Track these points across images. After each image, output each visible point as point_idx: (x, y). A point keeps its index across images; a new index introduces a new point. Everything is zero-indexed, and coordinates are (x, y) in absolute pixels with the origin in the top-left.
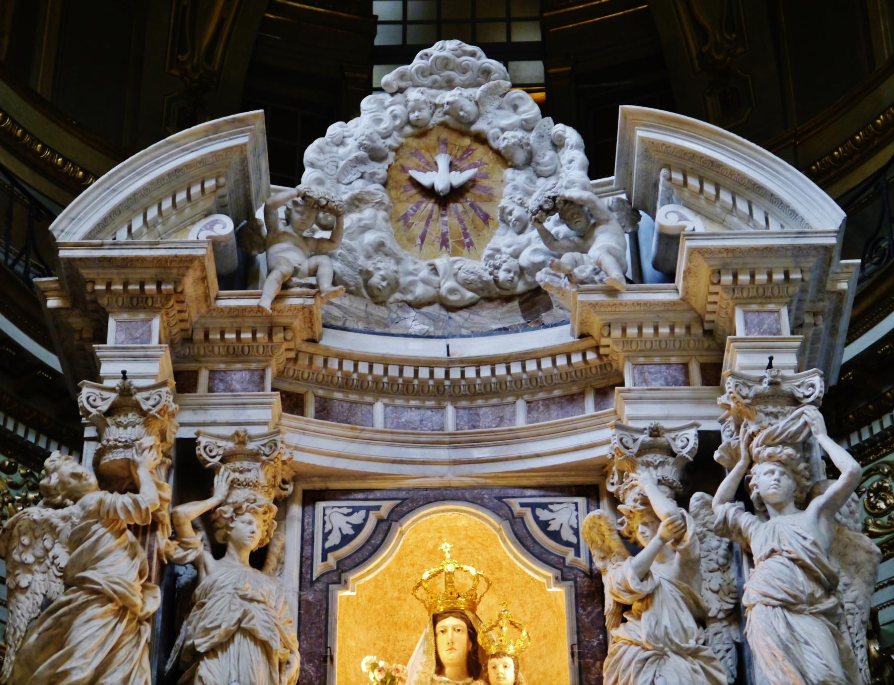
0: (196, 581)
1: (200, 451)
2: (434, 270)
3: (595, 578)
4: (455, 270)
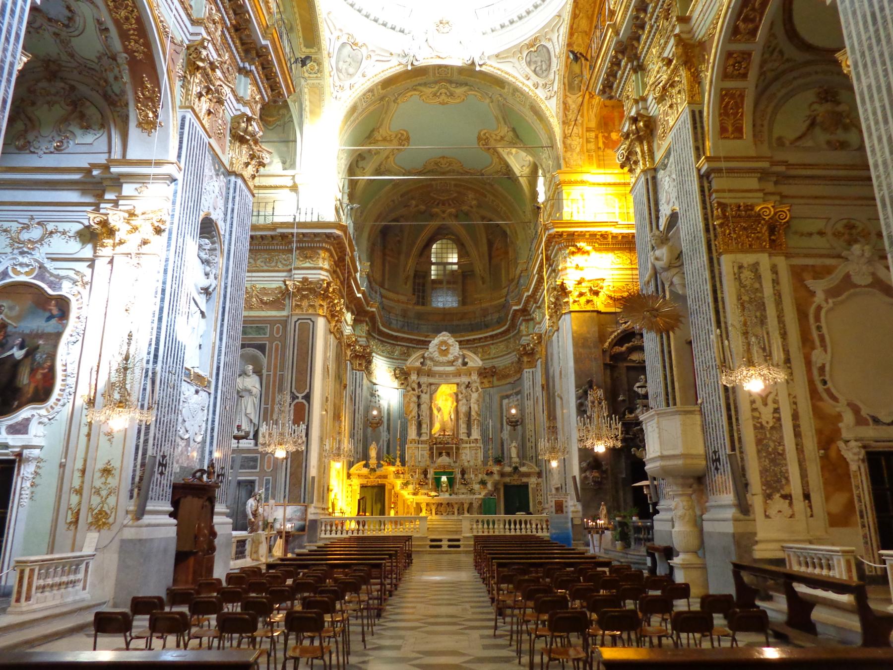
4: (444, 359)
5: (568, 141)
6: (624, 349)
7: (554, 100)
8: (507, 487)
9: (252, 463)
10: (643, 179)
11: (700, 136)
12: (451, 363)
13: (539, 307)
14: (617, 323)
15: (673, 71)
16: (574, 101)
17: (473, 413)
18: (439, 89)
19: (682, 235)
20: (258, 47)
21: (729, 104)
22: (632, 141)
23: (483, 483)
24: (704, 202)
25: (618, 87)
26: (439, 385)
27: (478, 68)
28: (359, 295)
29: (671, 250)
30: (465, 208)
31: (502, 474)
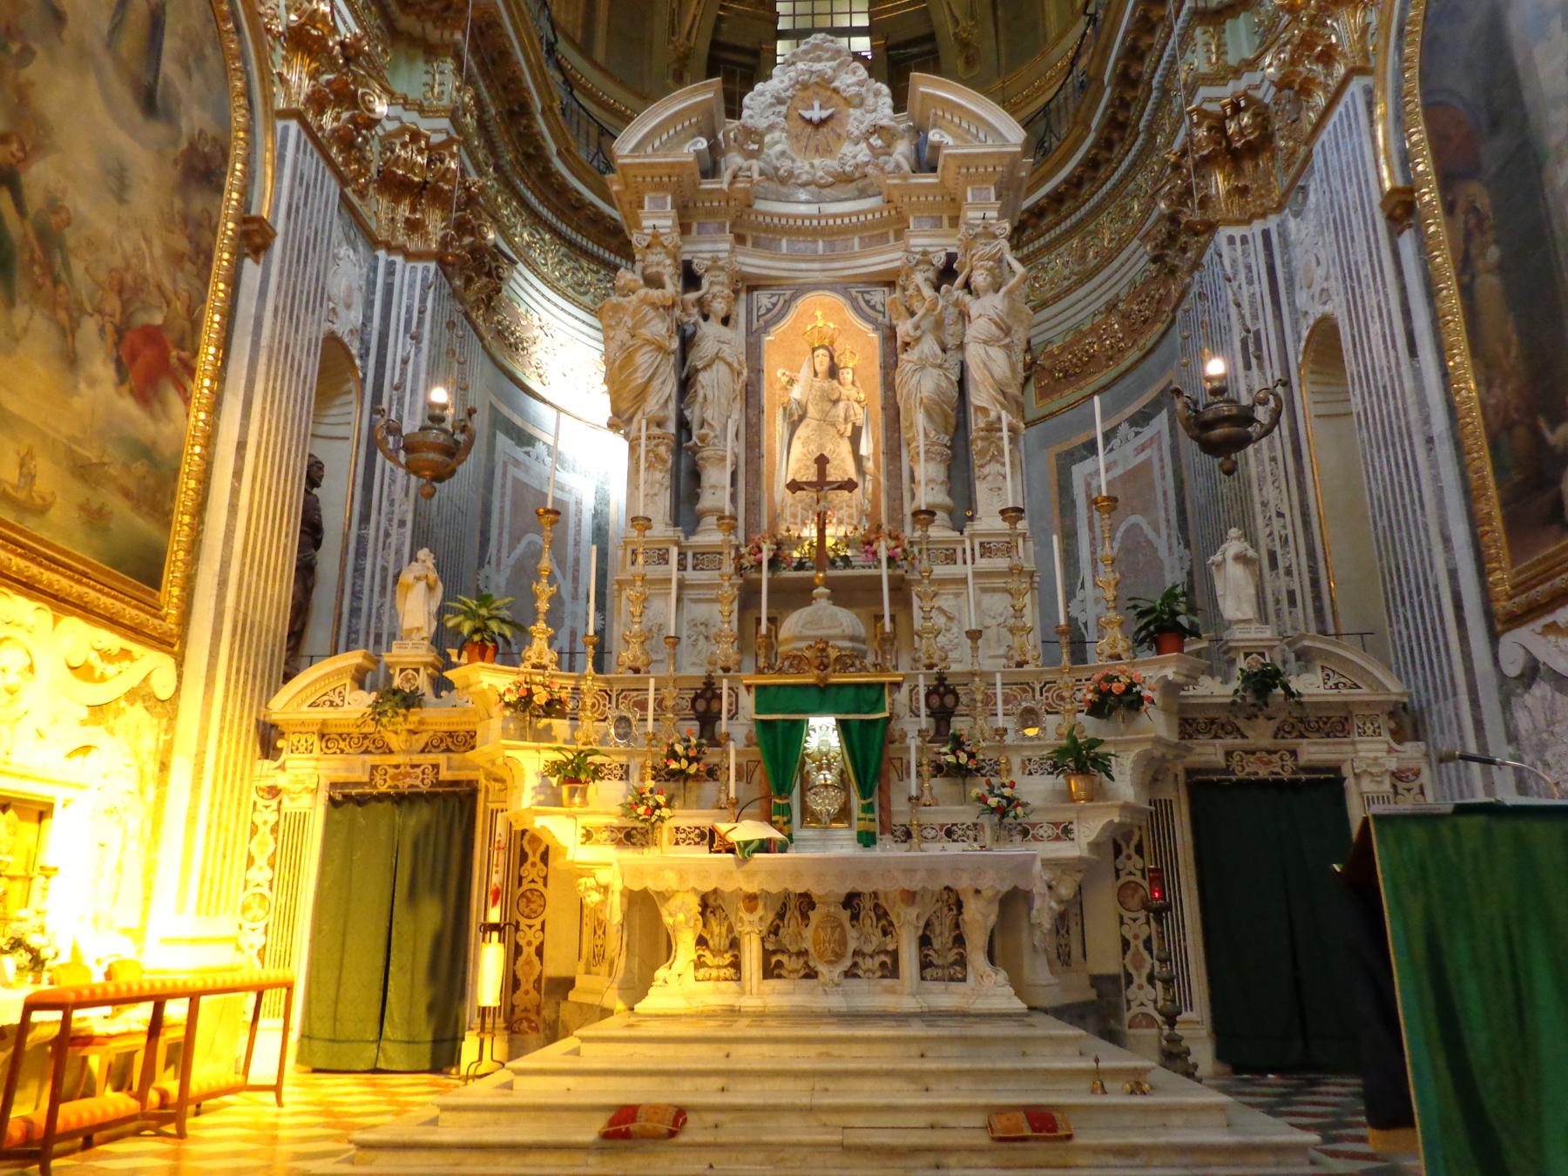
0: (694, 333)
1: (694, 266)
2: (812, 166)
3: (893, 329)
4: (823, 166)
17: (980, 396)
23: (1080, 760)
26: (801, 289)
31: (1191, 722)
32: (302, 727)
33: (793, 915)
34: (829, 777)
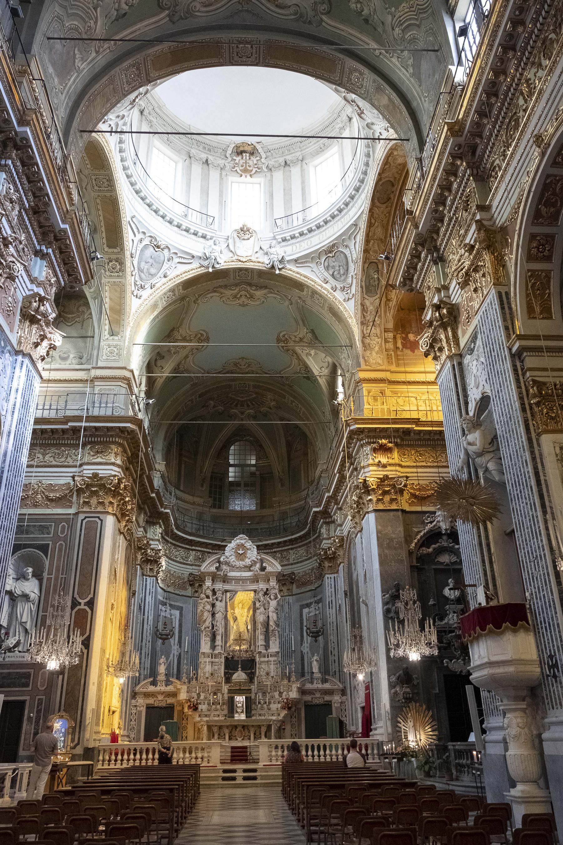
4: (242, 563)
5: (367, 341)
6: (431, 550)
7: (352, 302)
8: (309, 707)
9: (23, 680)
10: (449, 364)
11: (508, 316)
12: (248, 568)
13: (340, 509)
14: (423, 523)
15: (475, 258)
16: (372, 303)
17: (271, 623)
18: (240, 291)
19: (495, 417)
20: (57, 230)
21: (536, 285)
22: (435, 329)
24: (517, 381)
25: (418, 279)
26: (236, 592)
27: (277, 272)
28: (154, 495)
29: (484, 435)
30: (264, 409)
32: (141, 693)
33: (234, 729)
34: (240, 705)
